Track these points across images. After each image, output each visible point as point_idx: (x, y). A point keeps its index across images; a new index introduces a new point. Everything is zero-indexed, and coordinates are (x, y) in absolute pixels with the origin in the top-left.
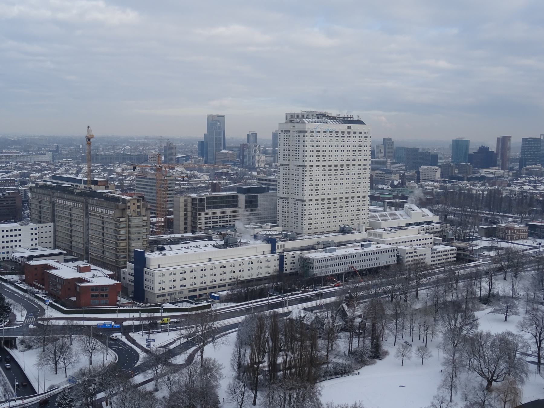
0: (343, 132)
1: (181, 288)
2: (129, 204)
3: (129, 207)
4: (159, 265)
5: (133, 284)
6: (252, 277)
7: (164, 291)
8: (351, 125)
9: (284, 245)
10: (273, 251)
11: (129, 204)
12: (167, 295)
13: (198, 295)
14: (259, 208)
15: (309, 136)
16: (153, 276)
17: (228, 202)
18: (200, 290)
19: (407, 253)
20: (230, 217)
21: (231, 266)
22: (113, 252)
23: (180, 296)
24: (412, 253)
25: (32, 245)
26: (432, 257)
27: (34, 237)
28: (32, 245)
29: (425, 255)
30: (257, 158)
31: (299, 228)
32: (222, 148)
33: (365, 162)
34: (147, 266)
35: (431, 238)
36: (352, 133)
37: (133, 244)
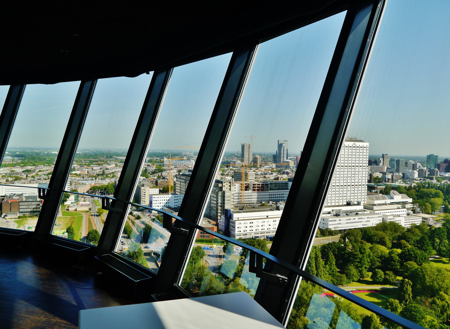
1: (250, 232)
3: (224, 185)
4: (238, 218)
5: (224, 228)
7: (240, 233)
12: (242, 235)
13: (259, 236)
16: (234, 224)
17: (279, 186)
19: (388, 219)
20: (283, 194)
22: (216, 210)
25: (175, 205)
27: (176, 201)
28: (175, 205)
29: (400, 221)
32: (285, 158)
35: (405, 211)
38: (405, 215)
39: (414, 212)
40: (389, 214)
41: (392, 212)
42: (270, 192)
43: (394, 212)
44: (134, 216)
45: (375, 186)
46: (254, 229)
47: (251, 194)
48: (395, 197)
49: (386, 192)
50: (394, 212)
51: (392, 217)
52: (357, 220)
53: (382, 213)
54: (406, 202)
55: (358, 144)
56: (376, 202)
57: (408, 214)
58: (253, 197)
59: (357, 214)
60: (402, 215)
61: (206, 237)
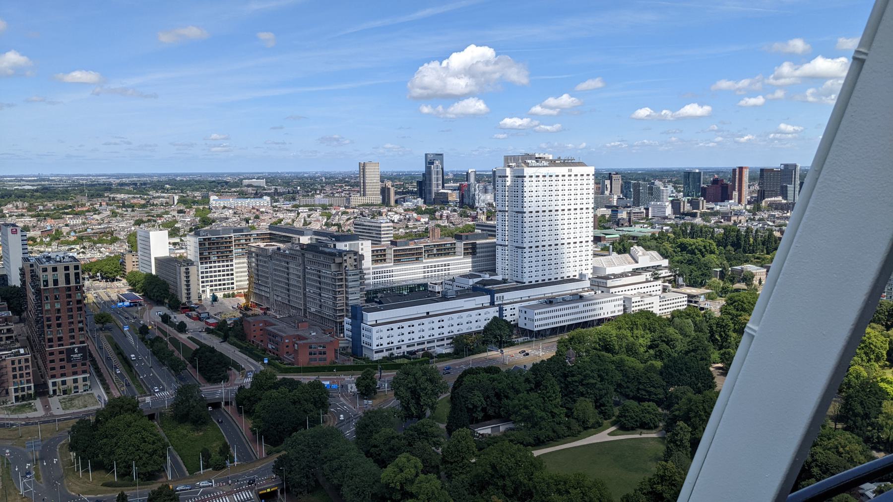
0: (564, 176)
1: (399, 344)
2: (345, 258)
3: (345, 260)
4: (376, 321)
6: (471, 331)
8: (573, 168)
9: (503, 297)
10: (492, 304)
11: (345, 258)
12: (385, 350)
14: (478, 255)
15: (527, 252)
16: (370, 332)
18: (418, 344)
21: (449, 326)
23: (398, 351)
24: (639, 302)
26: (660, 306)
29: (653, 303)
30: (477, 197)
31: (520, 276)
32: (440, 187)
33: (587, 206)
34: (364, 322)
36: (573, 176)
37: (351, 297)
38: (659, 293)
39: (674, 283)
40: (634, 292)
41: (638, 289)
42: (426, 263)
43: (641, 288)
44: (172, 325)
45: (602, 235)
46: (406, 338)
47: (391, 269)
48: (640, 259)
49: (622, 247)
50: (641, 288)
51: (639, 299)
52: (581, 308)
53: (622, 291)
54: (658, 266)
55: (576, 170)
56: (609, 271)
57: (665, 290)
58: (396, 273)
59: (581, 297)
60: (654, 293)
61: (320, 360)
